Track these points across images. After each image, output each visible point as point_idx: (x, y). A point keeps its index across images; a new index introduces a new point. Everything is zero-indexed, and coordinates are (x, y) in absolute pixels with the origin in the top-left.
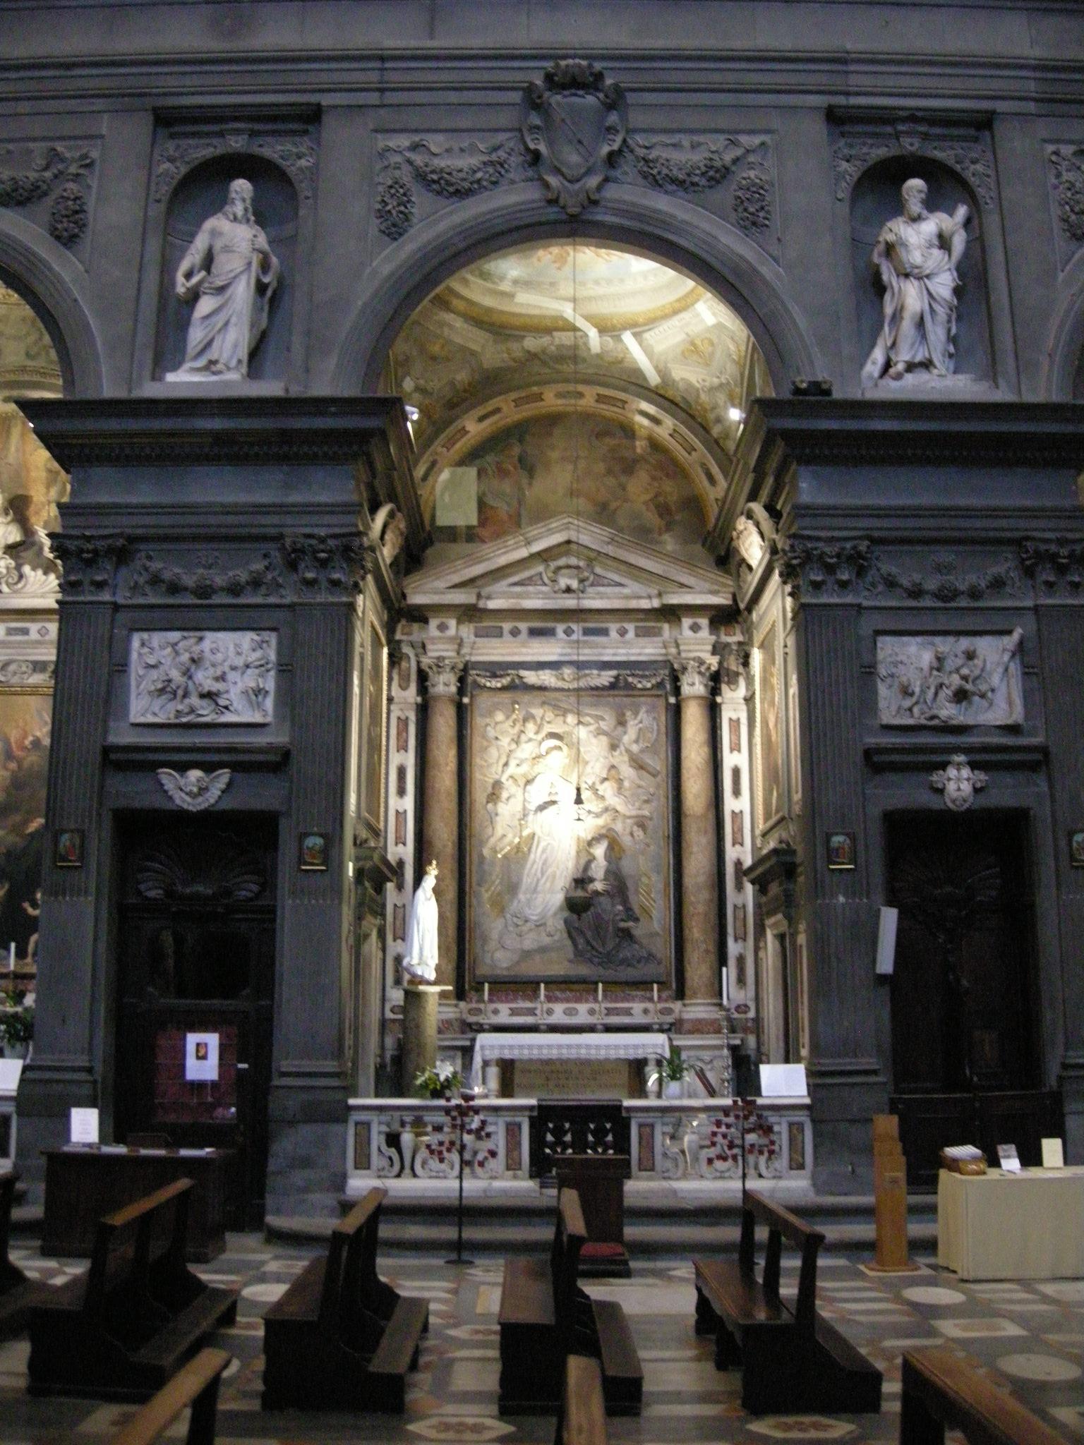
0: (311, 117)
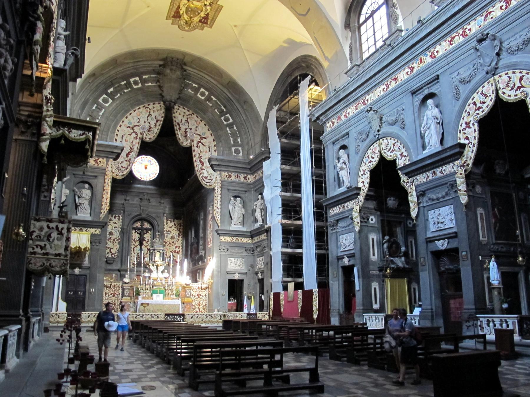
0: (438, 77)
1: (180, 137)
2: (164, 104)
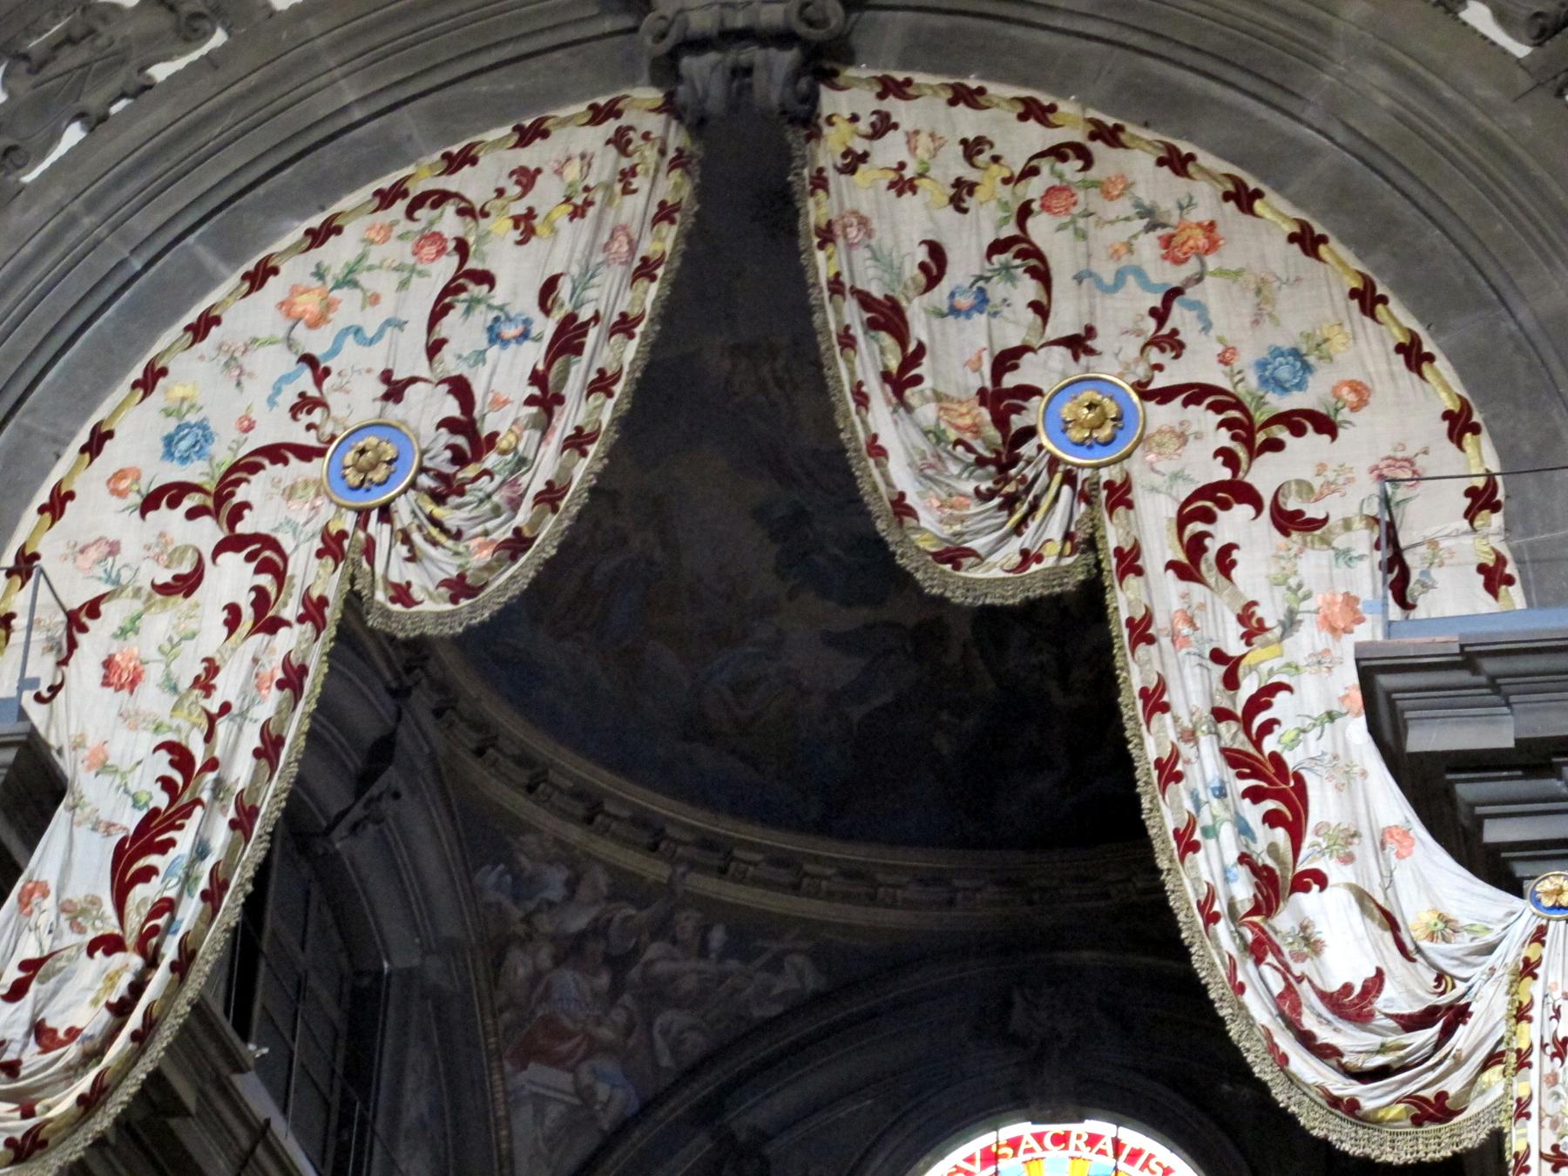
1: (901, 475)
2: (670, 107)
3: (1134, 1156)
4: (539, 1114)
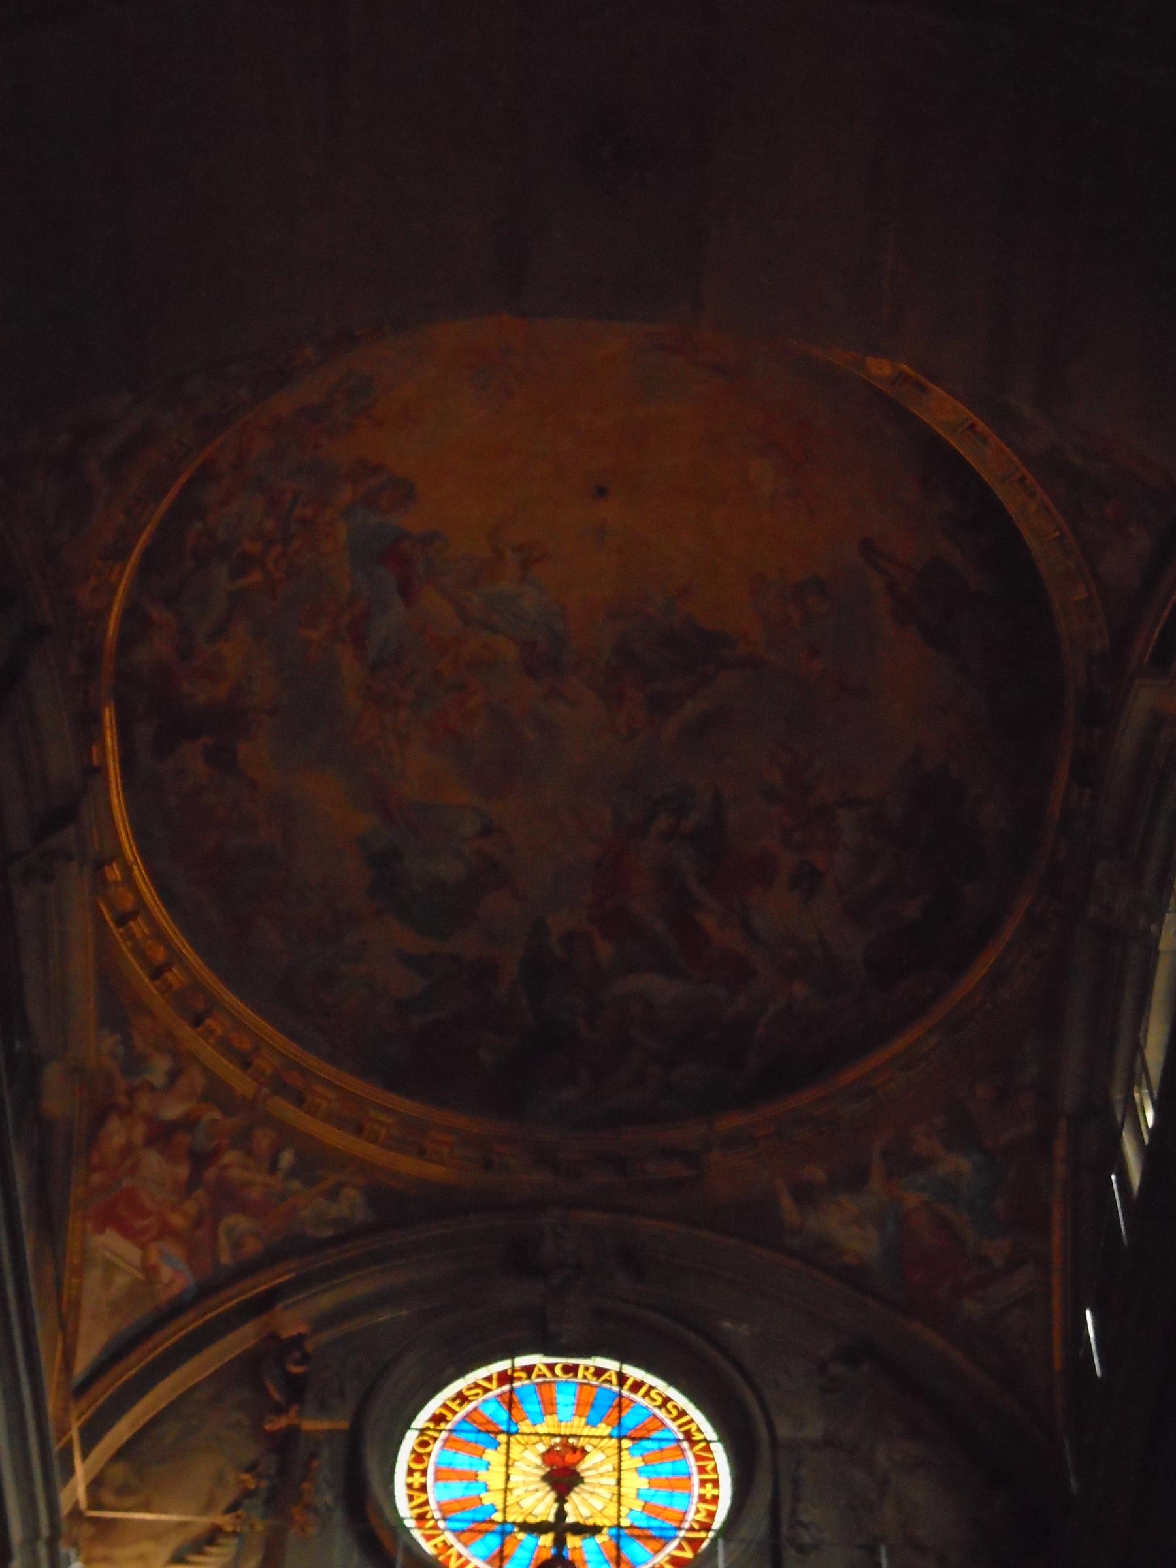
3: (637, 1386)
4: (107, 1282)
